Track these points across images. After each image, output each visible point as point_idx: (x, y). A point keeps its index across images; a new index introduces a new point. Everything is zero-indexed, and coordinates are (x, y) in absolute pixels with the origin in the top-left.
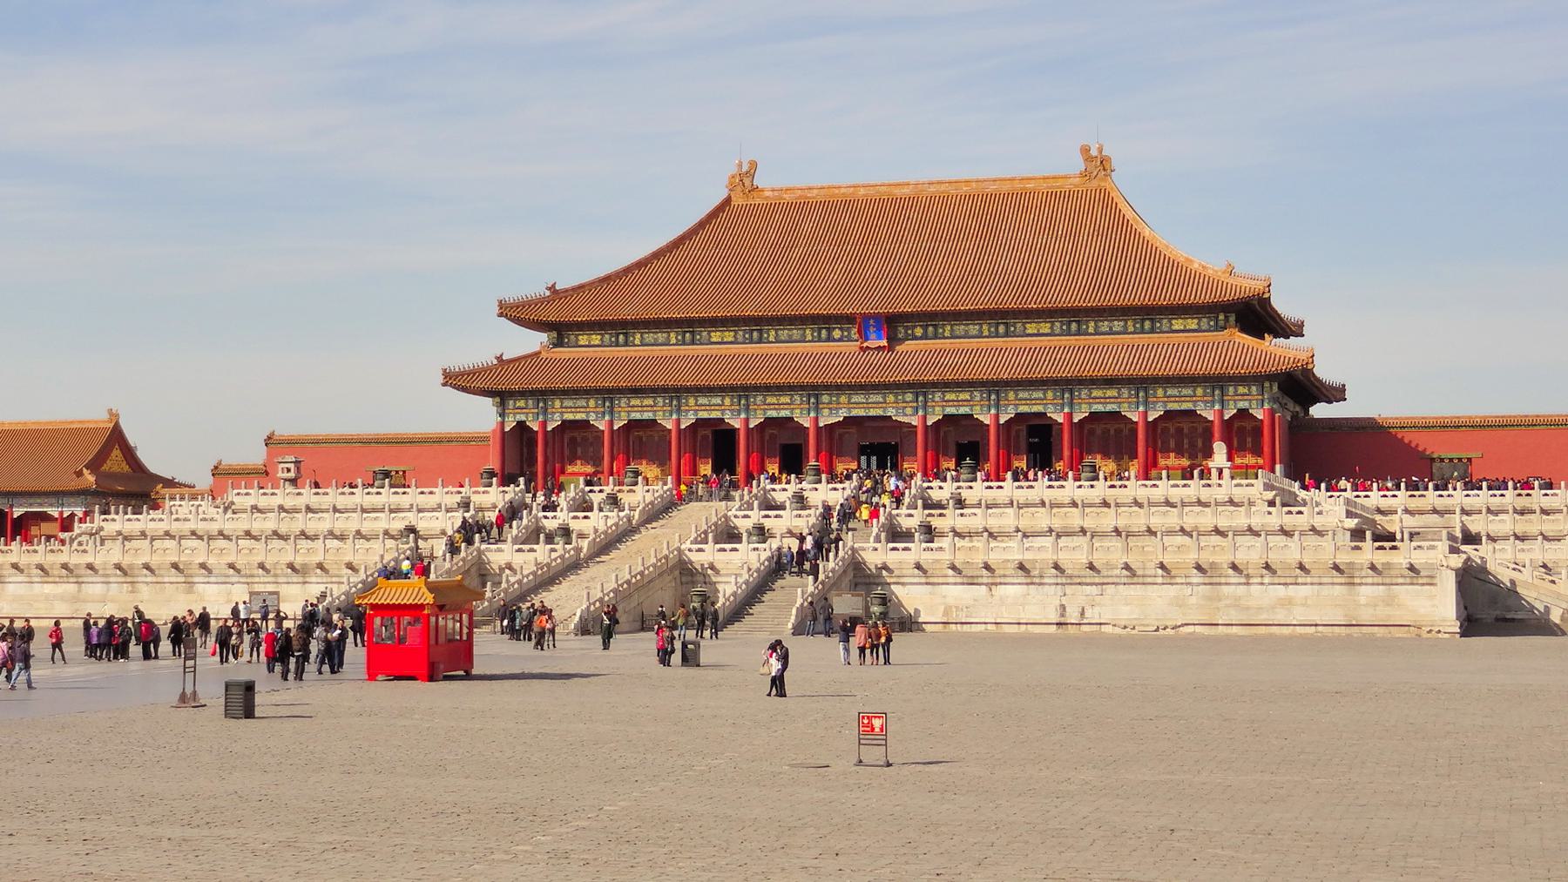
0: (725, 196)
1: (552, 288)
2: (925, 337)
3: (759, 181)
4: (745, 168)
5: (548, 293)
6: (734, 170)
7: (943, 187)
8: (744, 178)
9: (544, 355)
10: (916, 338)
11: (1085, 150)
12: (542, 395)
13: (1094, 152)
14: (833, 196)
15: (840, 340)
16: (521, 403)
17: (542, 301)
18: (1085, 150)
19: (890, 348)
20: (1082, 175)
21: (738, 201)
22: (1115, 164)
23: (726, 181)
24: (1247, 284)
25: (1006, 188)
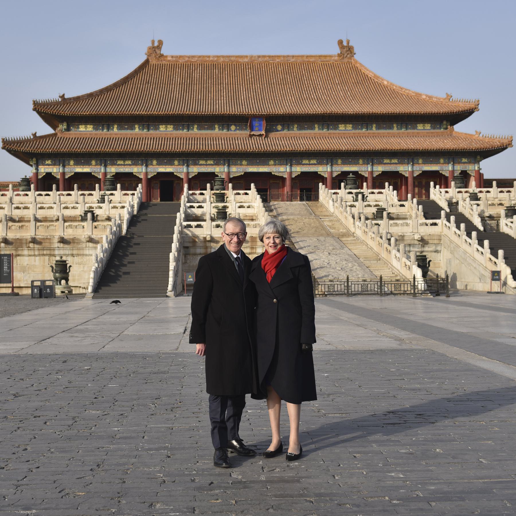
0: (144, 58)
1: (63, 97)
2: (283, 130)
3: (164, 51)
4: (156, 44)
5: (60, 100)
6: (150, 45)
7: (266, 59)
8: (155, 49)
9: (59, 135)
10: (278, 131)
11: (340, 42)
12: (60, 157)
13: (345, 44)
14: (206, 61)
15: (235, 130)
16: (49, 162)
17: (56, 103)
18: (340, 42)
19: (267, 136)
20: (339, 55)
21: (153, 61)
22: (356, 50)
23: (146, 50)
24: (461, 104)
25: (300, 60)
